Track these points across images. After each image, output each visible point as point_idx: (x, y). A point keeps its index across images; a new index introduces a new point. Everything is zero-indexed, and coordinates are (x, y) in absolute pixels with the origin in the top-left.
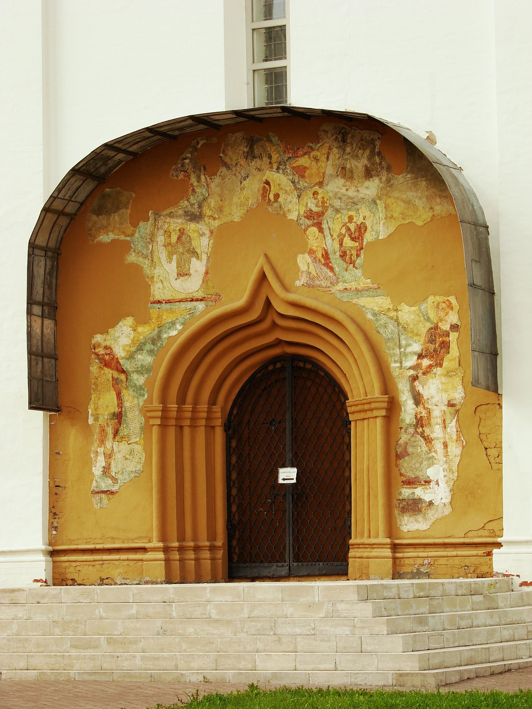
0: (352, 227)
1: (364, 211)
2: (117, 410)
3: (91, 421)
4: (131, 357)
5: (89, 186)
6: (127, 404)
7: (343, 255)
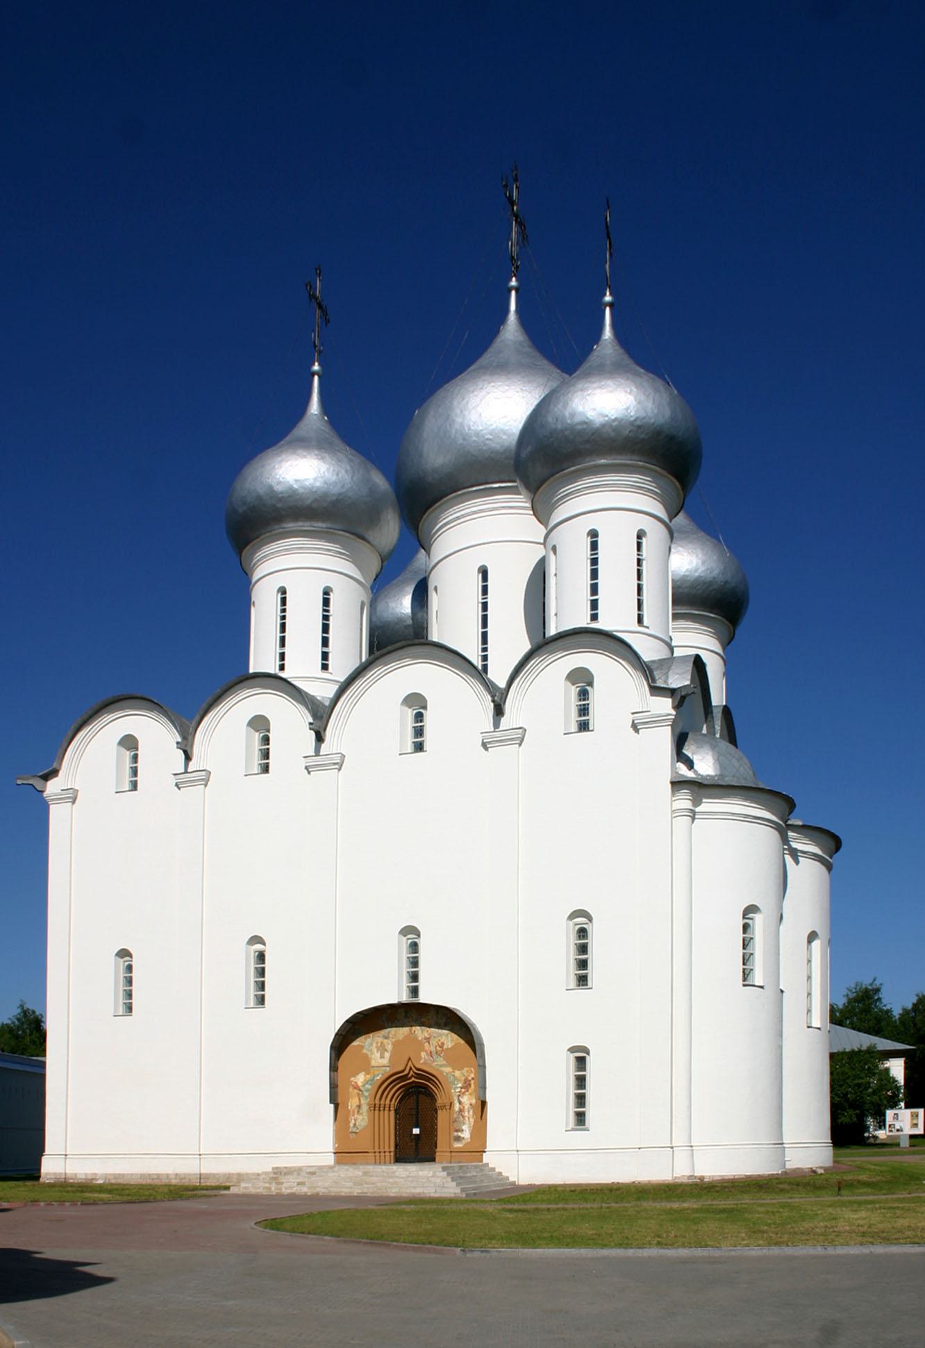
0: (440, 1043)
1: (444, 1037)
2: (358, 1104)
3: (349, 1107)
4: (364, 1086)
5: (351, 1025)
6: (362, 1102)
7: (437, 1052)
